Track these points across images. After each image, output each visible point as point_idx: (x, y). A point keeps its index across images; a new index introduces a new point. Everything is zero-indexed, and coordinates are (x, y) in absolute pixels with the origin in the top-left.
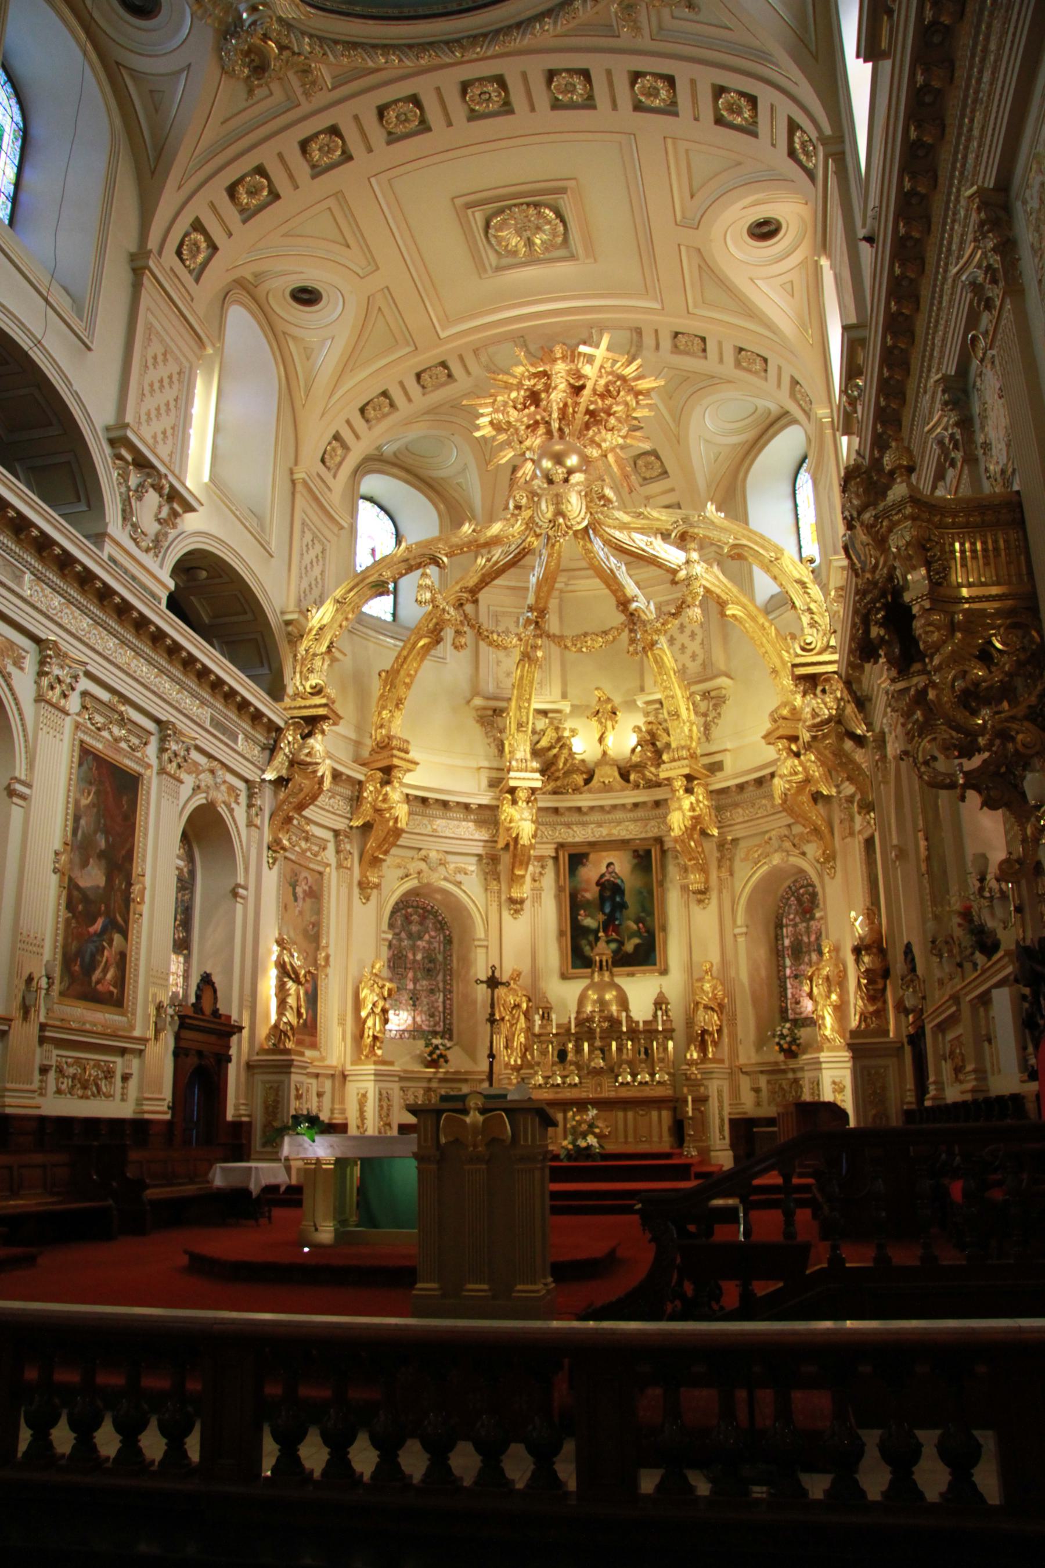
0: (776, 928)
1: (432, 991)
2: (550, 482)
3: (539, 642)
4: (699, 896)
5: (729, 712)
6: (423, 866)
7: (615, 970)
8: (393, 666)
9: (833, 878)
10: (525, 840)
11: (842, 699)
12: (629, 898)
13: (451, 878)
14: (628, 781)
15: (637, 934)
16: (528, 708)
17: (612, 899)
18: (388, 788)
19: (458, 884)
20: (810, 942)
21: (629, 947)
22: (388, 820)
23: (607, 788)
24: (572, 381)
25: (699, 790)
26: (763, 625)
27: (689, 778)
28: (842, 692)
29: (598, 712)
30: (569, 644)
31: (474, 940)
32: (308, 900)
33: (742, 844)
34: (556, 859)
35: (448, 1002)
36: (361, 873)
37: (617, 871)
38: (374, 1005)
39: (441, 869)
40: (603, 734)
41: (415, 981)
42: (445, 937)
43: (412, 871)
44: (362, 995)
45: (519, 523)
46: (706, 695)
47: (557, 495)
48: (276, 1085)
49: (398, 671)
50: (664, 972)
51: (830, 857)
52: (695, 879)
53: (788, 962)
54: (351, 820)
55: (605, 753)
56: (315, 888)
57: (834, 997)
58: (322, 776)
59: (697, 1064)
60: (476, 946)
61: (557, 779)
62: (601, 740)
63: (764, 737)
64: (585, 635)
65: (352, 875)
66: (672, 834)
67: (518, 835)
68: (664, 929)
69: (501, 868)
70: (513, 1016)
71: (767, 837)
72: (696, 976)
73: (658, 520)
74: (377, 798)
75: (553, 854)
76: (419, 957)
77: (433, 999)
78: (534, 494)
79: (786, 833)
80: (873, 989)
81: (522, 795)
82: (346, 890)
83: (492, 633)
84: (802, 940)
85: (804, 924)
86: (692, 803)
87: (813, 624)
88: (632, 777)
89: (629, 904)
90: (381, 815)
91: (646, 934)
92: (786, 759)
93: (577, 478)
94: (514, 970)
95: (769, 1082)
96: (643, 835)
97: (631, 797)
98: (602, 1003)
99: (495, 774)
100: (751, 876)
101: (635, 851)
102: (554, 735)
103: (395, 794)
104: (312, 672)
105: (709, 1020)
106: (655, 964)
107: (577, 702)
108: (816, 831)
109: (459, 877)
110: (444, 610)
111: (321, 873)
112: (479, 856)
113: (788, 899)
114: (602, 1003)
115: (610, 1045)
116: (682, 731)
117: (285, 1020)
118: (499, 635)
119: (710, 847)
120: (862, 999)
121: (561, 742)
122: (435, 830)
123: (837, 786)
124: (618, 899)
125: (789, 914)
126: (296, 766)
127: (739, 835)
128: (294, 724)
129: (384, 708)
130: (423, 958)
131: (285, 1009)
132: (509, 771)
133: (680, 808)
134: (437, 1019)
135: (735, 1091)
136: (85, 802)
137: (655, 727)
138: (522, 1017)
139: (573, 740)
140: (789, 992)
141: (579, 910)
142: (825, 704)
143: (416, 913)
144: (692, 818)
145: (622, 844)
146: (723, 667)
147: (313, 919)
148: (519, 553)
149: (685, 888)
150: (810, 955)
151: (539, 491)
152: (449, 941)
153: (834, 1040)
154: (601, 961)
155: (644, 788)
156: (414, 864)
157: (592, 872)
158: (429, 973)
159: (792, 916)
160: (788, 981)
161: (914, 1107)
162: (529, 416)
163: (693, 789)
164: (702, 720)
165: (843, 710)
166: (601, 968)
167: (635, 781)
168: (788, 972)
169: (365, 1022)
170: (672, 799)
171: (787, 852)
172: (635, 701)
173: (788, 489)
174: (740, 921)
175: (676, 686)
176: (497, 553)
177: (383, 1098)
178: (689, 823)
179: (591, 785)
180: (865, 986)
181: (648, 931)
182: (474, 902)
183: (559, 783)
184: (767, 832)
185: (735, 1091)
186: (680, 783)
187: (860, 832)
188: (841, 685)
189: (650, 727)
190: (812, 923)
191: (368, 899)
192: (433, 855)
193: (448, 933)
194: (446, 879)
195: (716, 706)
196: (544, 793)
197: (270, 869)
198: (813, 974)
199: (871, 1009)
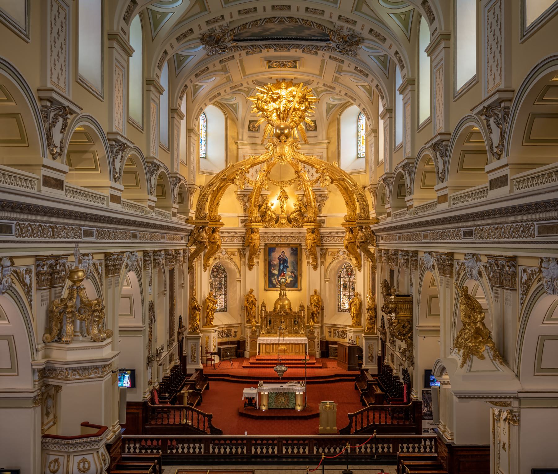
1: (220, 295)
6: (220, 254)
12: (289, 264)
14: (291, 224)
15: (292, 277)
21: (288, 281)
24: (288, 99)
33: (329, 250)
43: (217, 257)
49: (218, 193)
50: (300, 290)
51: (359, 267)
53: (342, 290)
61: (266, 222)
63: (342, 225)
65: (201, 263)
68: (301, 275)
76: (217, 284)
94: (251, 290)
95: (334, 330)
96: (295, 242)
98: (283, 307)
102: (265, 206)
106: (297, 287)
108: (356, 258)
109: (231, 257)
112: (239, 249)
113: (343, 269)
122: (224, 241)
124: (285, 264)
132: (251, 221)
140: (341, 299)
145: (289, 245)
152: (226, 277)
155: (296, 227)
157: (276, 255)
158: (220, 289)
161: (381, 355)
168: (341, 293)
173: (356, 119)
181: (295, 276)
185: (322, 332)
192: (224, 250)
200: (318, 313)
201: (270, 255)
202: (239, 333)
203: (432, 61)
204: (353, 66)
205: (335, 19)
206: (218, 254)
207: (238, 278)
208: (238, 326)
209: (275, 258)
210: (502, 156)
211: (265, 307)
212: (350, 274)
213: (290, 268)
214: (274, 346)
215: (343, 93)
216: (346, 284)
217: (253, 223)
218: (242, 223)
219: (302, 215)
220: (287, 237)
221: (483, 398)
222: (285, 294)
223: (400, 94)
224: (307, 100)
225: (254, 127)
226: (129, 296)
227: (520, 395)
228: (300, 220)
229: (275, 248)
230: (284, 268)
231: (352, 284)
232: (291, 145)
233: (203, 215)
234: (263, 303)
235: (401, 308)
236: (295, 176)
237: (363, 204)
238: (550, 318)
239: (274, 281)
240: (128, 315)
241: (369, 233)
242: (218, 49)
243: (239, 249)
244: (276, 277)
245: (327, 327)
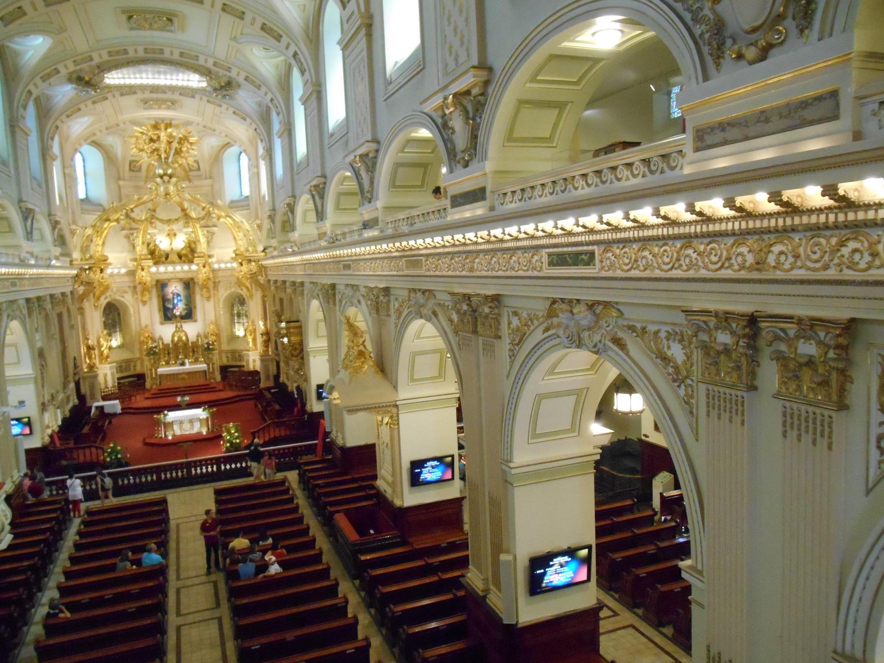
1: (115, 332)
6: (111, 293)
19: (123, 297)
23: (173, 263)
34: (156, 285)
41: (110, 330)
46: (208, 232)
50: (196, 321)
51: (251, 296)
52: (206, 294)
53: (236, 318)
55: (172, 249)
62: (171, 244)
64: (170, 220)
68: (195, 307)
93: (174, 180)
98: (180, 338)
99: (132, 257)
108: (247, 288)
112: (129, 287)
114: (180, 338)
119: (211, 285)
135: (221, 358)
149: (202, 295)
152: (119, 314)
162: (151, 147)
174: (221, 306)
177: (112, 374)
185: (221, 358)
192: (114, 289)
195: (212, 236)
203: (305, 110)
204: (231, 110)
205: (210, 65)
206: (108, 294)
210: (372, 200)
211: (162, 339)
212: (242, 302)
215: (223, 135)
219: (193, 251)
221: (368, 408)
222: (181, 326)
223: (279, 137)
224: (188, 141)
225: (134, 166)
226: (15, 345)
227: (398, 403)
232: (176, 185)
235: (292, 333)
238: (418, 337)
240: (15, 364)
242: (89, 90)
243: (129, 287)
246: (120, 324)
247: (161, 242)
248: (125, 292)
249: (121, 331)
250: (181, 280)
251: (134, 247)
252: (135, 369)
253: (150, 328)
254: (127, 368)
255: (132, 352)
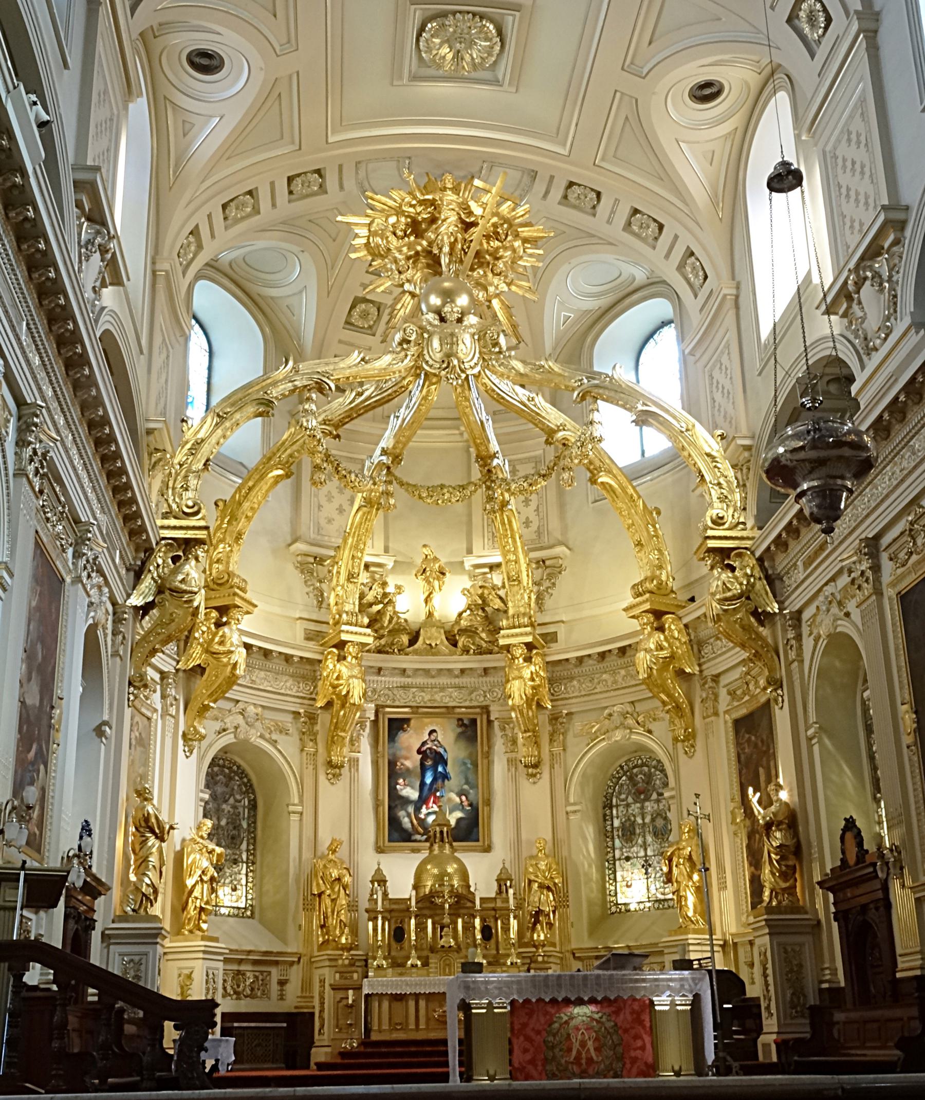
0: (604, 808)
1: (235, 862)
2: (442, 319)
3: (391, 488)
4: (530, 770)
5: (564, 582)
6: (240, 720)
7: (455, 844)
8: (233, 496)
9: (691, 757)
10: (356, 697)
11: (752, 576)
13: (267, 736)
14: (455, 645)
16: (360, 559)
17: (435, 770)
18: (226, 629)
19: (274, 743)
20: (644, 824)
22: (226, 665)
23: (431, 650)
25: (537, 660)
26: (632, 496)
27: (530, 646)
28: (752, 569)
29: (425, 570)
30: (424, 495)
31: (288, 805)
32: (138, 748)
34: (375, 722)
35: (251, 874)
36: (186, 722)
37: (439, 739)
38: (203, 872)
39: (258, 724)
40: (431, 593)
42: (249, 802)
43: (228, 725)
44: (188, 861)
45: (409, 358)
47: (452, 335)
48: (137, 958)
49: (240, 504)
50: (488, 849)
51: (690, 737)
52: (525, 752)
54: (178, 662)
55: (430, 615)
56: (144, 735)
57: (696, 877)
58: (198, 608)
59: (544, 946)
60: (289, 813)
63: (624, 610)
64: (442, 486)
66: (510, 702)
67: (348, 692)
68: (488, 803)
69: (318, 727)
70: (332, 889)
71: (607, 712)
72: (525, 854)
73: (560, 375)
74: (213, 639)
75: (373, 718)
76: (223, 822)
77: (236, 870)
78: (423, 329)
79: (629, 710)
80: (787, 866)
81: (351, 649)
82: (171, 740)
83: (350, 473)
84: (635, 821)
85: (638, 805)
86: (532, 673)
87: (723, 499)
88: (462, 641)
89: (452, 775)
90: (217, 659)
91: (469, 808)
92: (650, 635)
93: (472, 320)
94: (333, 840)
96: (467, 704)
97: (459, 662)
99: (313, 627)
100: (586, 752)
101: (460, 720)
103: (233, 636)
104: (187, 490)
105: (547, 901)
106: (478, 840)
107: (399, 559)
109: (274, 737)
110: (319, 440)
111: (149, 719)
113: (620, 778)
115: (456, 923)
116: (523, 598)
117: (147, 880)
118: (357, 476)
119: (543, 718)
120: (773, 874)
121: (386, 600)
122: (253, 682)
123: (700, 665)
124: (440, 769)
125: (620, 793)
126: (167, 593)
127: (573, 710)
128: (166, 545)
129: (222, 541)
130: (228, 823)
131: (147, 868)
132: (337, 623)
133: (521, 677)
134: (239, 892)
136: (34, 604)
137: (486, 592)
138: (342, 891)
139: (398, 597)
140: (619, 874)
141: (398, 779)
142: (736, 578)
143: (222, 772)
144: (533, 688)
146: (560, 537)
147: (141, 771)
148: (395, 391)
149: (512, 762)
150: (644, 837)
151: (429, 328)
152: (253, 806)
153: (698, 922)
154: (442, 832)
156: (231, 718)
159: (623, 796)
160: (617, 863)
163: (531, 658)
164: (535, 589)
165: (753, 585)
166: (442, 840)
167: (464, 646)
168: (617, 854)
169: (191, 892)
170: (510, 667)
171: (630, 729)
172: (463, 562)
175: (520, 550)
176: (369, 390)
178: (529, 691)
179: (416, 646)
180: (777, 861)
181: (470, 805)
182: (289, 763)
183: (383, 641)
184: (606, 707)
186: (520, 651)
187: (726, 712)
188: (752, 562)
189: (480, 591)
190: (647, 804)
191: (191, 753)
192: (251, 710)
193: (252, 797)
194: (262, 736)
195: (550, 576)
196: (368, 651)
197: (129, 706)
198: (673, 854)
199: (784, 885)
200: (554, 912)
201: (392, 737)
202: (293, 989)
207: (294, 805)
208: (292, 964)
209: (409, 748)
211: (382, 882)
213: (455, 780)
214: (422, 1003)
216: (633, 823)
217: (344, 628)
218: (308, 639)
220: (442, 689)
228: (484, 635)
229: (407, 721)
230: (435, 780)
231: (653, 820)
233: (190, 503)
234: (379, 870)
236: (476, 473)
237: (719, 484)
239: (406, 820)
241: (749, 571)
244: (411, 809)
245: (579, 959)
246: (253, 841)
247: (399, 587)
248: (283, 731)
249: (251, 862)
250: (450, 709)
251: (321, 601)
252: (282, 997)
253: (343, 852)
254: (259, 989)
255: (282, 936)
